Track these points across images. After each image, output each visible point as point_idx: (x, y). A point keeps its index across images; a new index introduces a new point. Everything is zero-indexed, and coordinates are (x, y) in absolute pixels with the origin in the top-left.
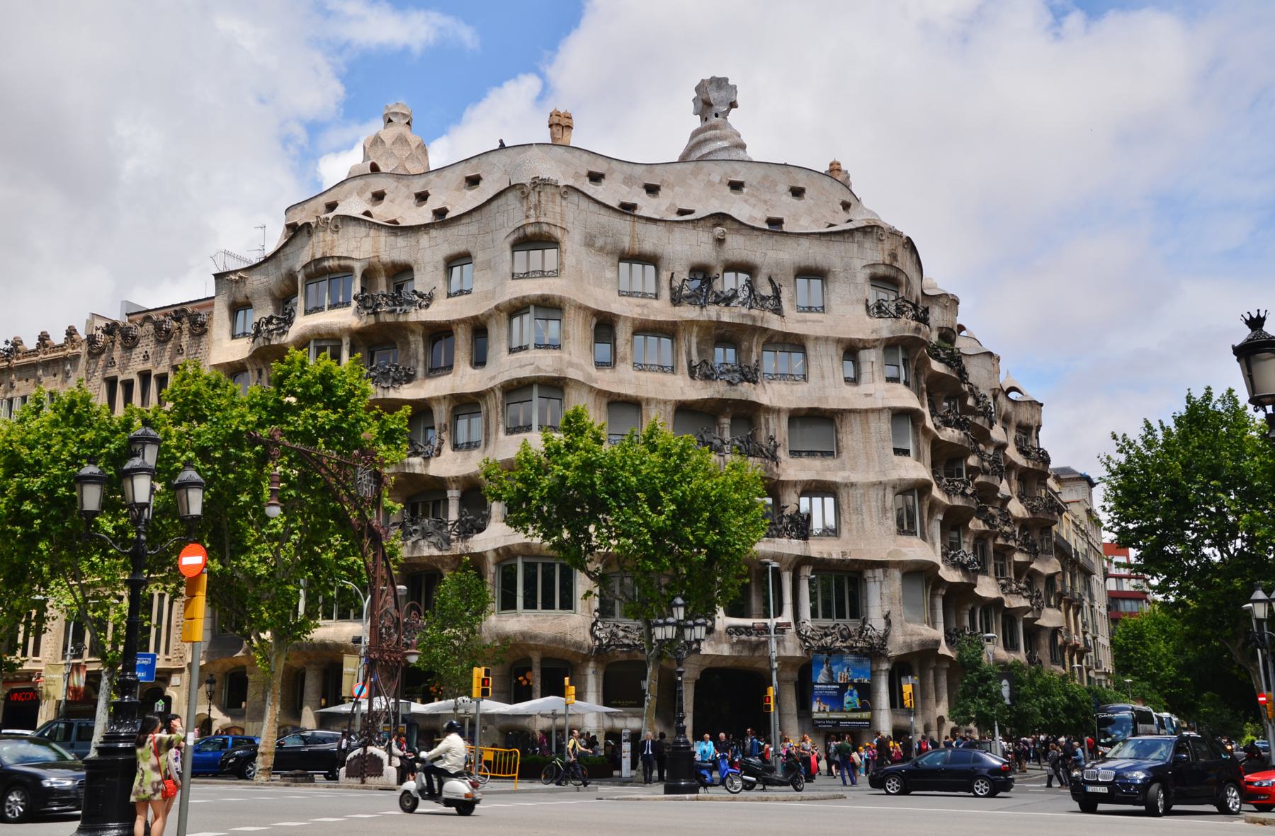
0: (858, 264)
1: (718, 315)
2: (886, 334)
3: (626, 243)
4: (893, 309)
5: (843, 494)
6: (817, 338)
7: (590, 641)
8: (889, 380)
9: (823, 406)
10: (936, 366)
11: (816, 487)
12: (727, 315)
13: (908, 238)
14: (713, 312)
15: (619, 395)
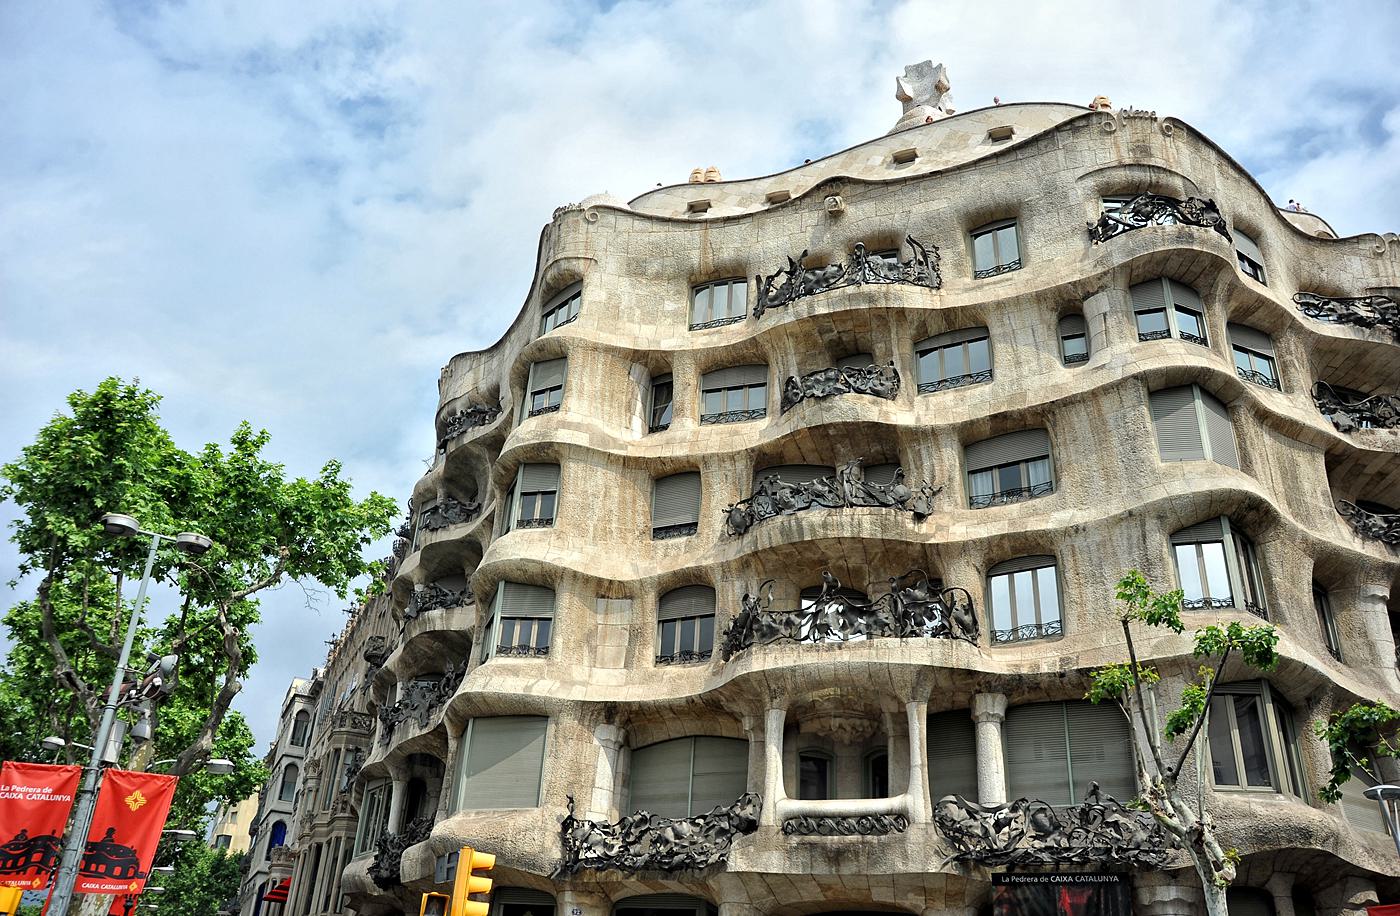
0: (1067, 177)
1: (811, 306)
2: (1118, 260)
3: (695, 258)
4: (1128, 218)
5: (1062, 548)
6: (1000, 305)
7: (556, 854)
8: (1143, 338)
9: (1016, 408)
10: (1329, 329)
11: (1014, 550)
12: (822, 305)
13: (1168, 119)
14: (801, 307)
15: (661, 461)
